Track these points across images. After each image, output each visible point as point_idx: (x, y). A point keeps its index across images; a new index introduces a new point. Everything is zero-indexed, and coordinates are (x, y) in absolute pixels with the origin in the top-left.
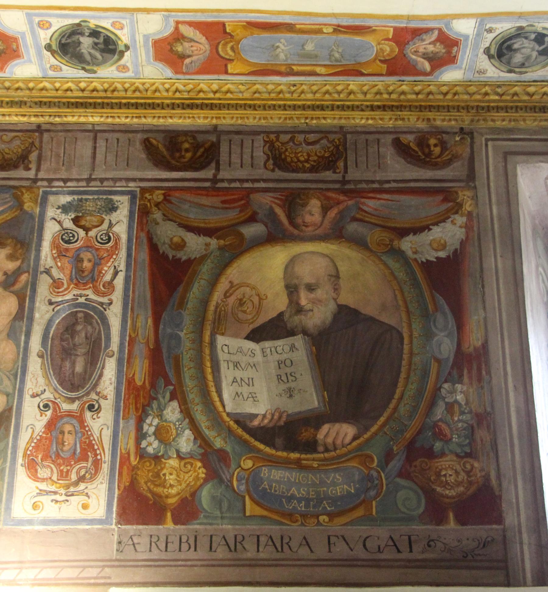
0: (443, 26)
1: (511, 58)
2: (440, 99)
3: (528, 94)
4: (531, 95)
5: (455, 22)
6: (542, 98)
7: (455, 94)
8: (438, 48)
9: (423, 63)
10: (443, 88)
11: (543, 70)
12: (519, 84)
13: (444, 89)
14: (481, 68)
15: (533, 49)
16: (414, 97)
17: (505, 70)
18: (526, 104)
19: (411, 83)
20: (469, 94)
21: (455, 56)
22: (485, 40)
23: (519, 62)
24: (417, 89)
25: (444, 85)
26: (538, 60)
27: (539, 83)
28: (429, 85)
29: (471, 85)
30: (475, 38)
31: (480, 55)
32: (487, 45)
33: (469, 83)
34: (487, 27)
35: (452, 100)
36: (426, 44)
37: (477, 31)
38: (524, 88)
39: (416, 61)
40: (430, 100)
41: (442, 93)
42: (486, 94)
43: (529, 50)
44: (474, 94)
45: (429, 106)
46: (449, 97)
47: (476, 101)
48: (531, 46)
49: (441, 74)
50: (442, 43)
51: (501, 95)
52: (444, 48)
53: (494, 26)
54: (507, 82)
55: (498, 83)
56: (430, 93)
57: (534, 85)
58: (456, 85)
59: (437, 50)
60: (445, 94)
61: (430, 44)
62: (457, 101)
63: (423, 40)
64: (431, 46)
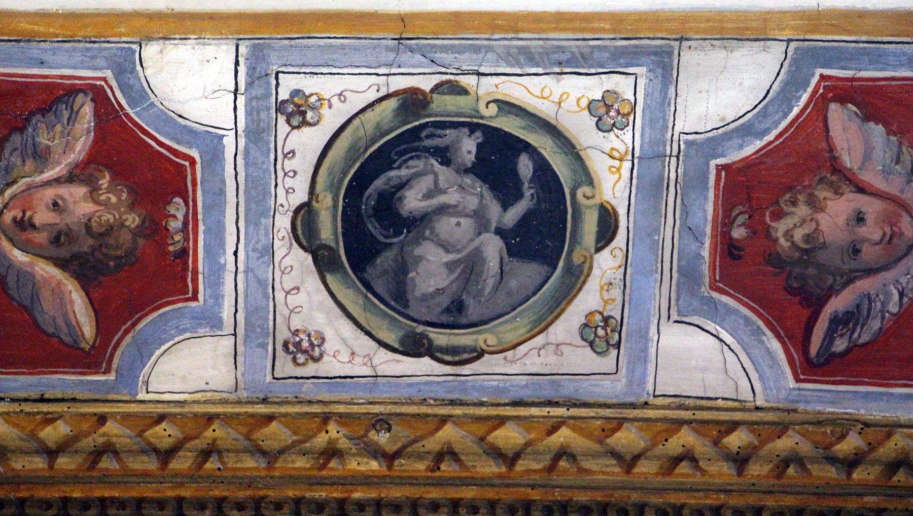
0: (108, 74)
1: (402, 270)
2: (146, 474)
3: (496, 453)
4: (511, 459)
5: (151, 51)
6: (551, 468)
7: (206, 454)
8: (106, 204)
9: (58, 292)
10: (159, 429)
11: (539, 340)
12: (458, 411)
13: (165, 434)
14: (296, 324)
15: (482, 226)
16: (39, 463)
17: (391, 338)
18: (491, 494)
19: (28, 408)
20: (264, 453)
21: (183, 253)
22: (289, 165)
23: (439, 291)
24: (53, 434)
25: (161, 418)
26: (513, 283)
27: (534, 411)
28: (102, 419)
29: (270, 418)
30: (247, 151)
31: (280, 248)
32: (300, 196)
33: (262, 409)
34: (284, 95)
35: (193, 476)
36: (58, 181)
37: (249, 113)
38: (481, 429)
39: (25, 276)
40: (106, 478)
41: (156, 451)
42: (332, 452)
43: (467, 223)
44: (282, 452)
45: (102, 500)
46: (182, 463)
47: (292, 479)
48: (472, 203)
49: (143, 354)
50: (120, 174)
51: (390, 458)
52: (132, 207)
53: (309, 85)
54: (411, 402)
55: (377, 409)
56: (108, 449)
57: (518, 418)
58: (210, 418)
59: (108, 217)
60: (166, 455)
61: (71, 178)
62: (213, 479)
63: (42, 157)
64: (80, 191)
